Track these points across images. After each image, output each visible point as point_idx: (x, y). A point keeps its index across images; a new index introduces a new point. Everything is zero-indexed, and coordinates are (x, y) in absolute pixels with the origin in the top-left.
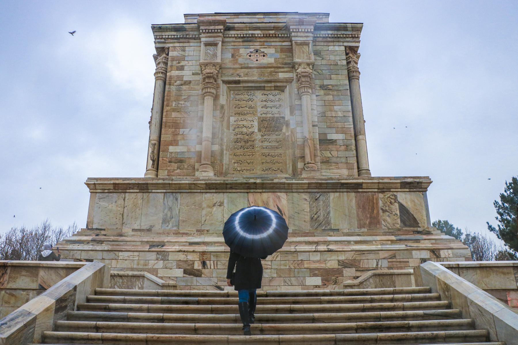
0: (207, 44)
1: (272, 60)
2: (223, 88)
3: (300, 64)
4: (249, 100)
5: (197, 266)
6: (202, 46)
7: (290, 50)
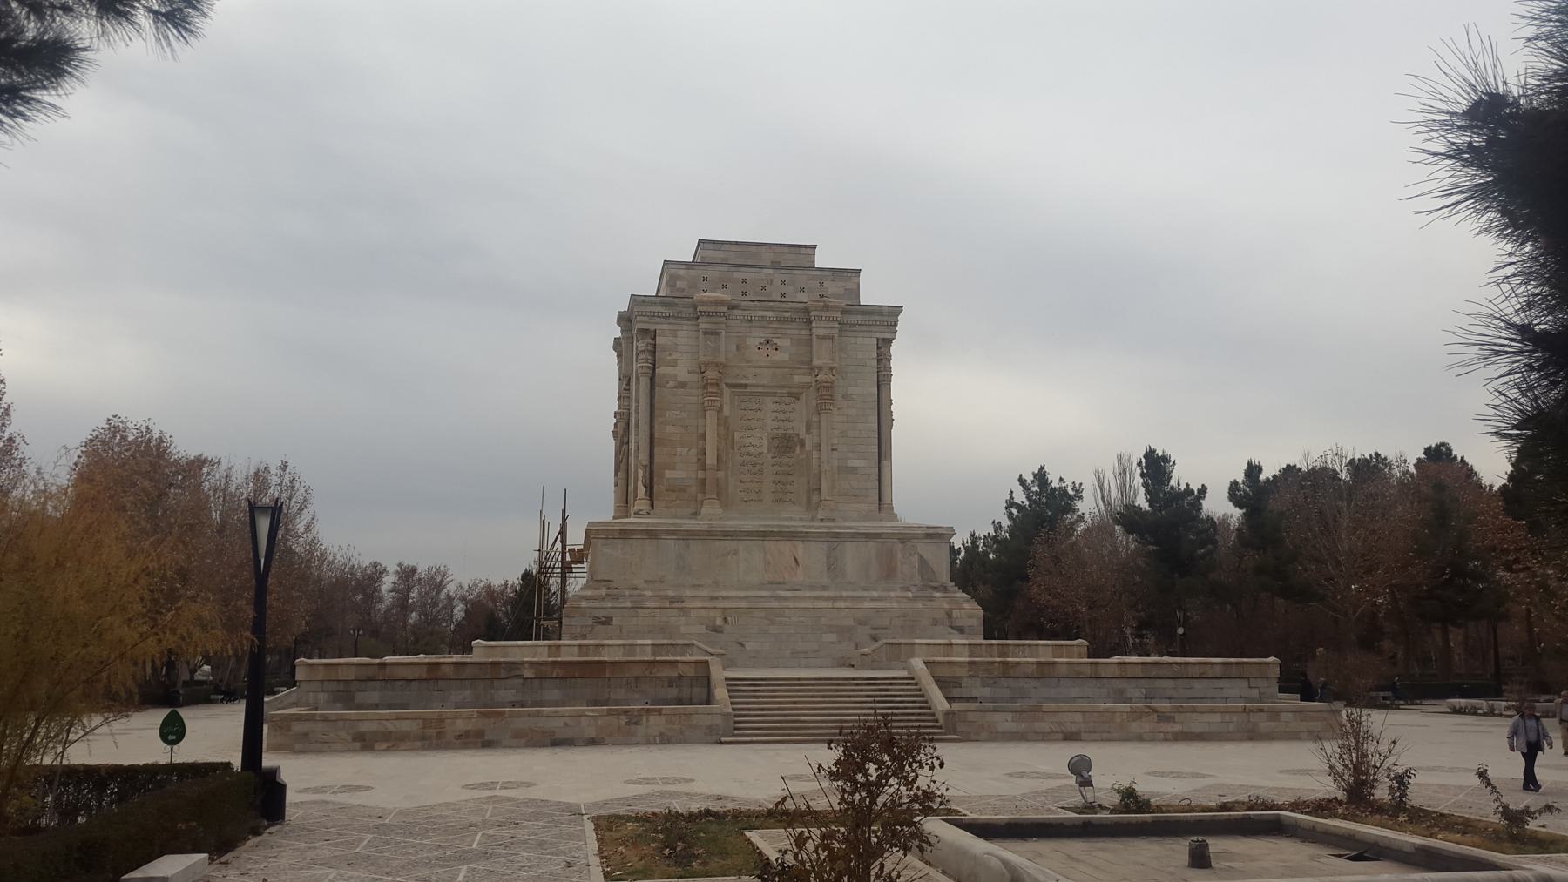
0: (705, 333)
1: (786, 357)
2: (727, 391)
3: (820, 369)
4: (759, 409)
5: (719, 622)
6: (701, 336)
7: (809, 342)
